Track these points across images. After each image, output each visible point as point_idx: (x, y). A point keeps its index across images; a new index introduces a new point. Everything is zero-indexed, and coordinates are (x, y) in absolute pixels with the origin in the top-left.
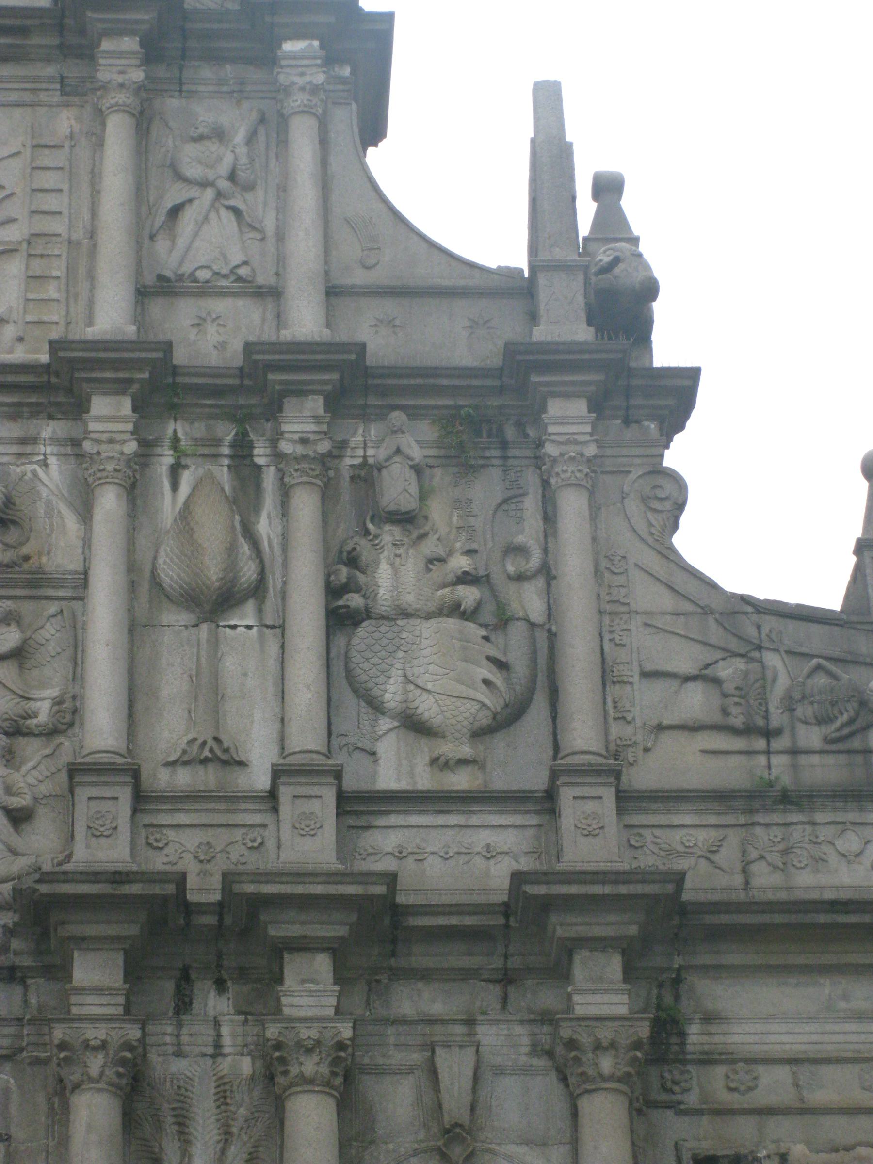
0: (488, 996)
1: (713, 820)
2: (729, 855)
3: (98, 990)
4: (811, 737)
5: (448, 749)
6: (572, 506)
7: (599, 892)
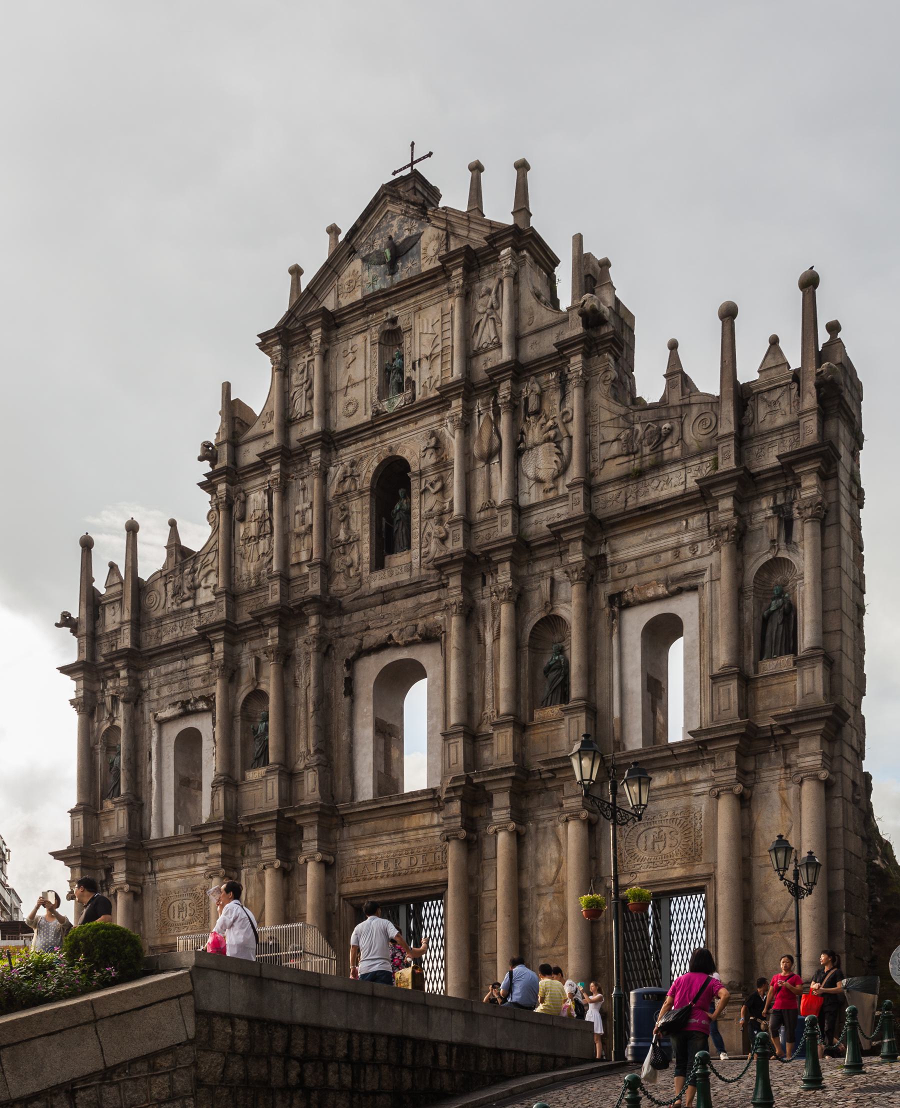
1: (617, 487)
2: (622, 497)
3: (455, 587)
5: (549, 485)
7: (570, 524)
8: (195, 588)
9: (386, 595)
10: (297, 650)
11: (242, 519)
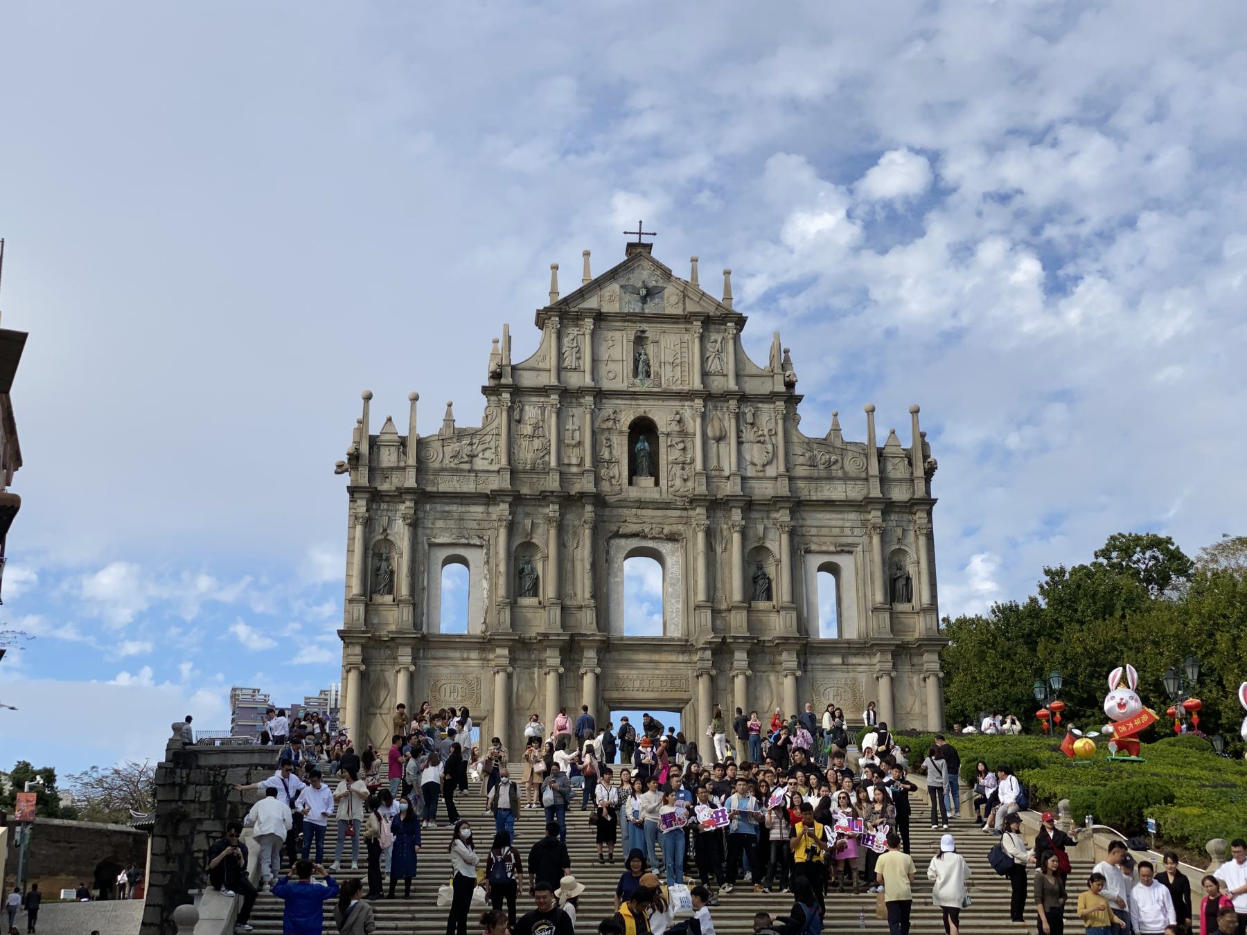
0: (765, 515)
4: (821, 467)
5: (759, 468)
8: (472, 457)
9: (641, 504)
10: (565, 522)
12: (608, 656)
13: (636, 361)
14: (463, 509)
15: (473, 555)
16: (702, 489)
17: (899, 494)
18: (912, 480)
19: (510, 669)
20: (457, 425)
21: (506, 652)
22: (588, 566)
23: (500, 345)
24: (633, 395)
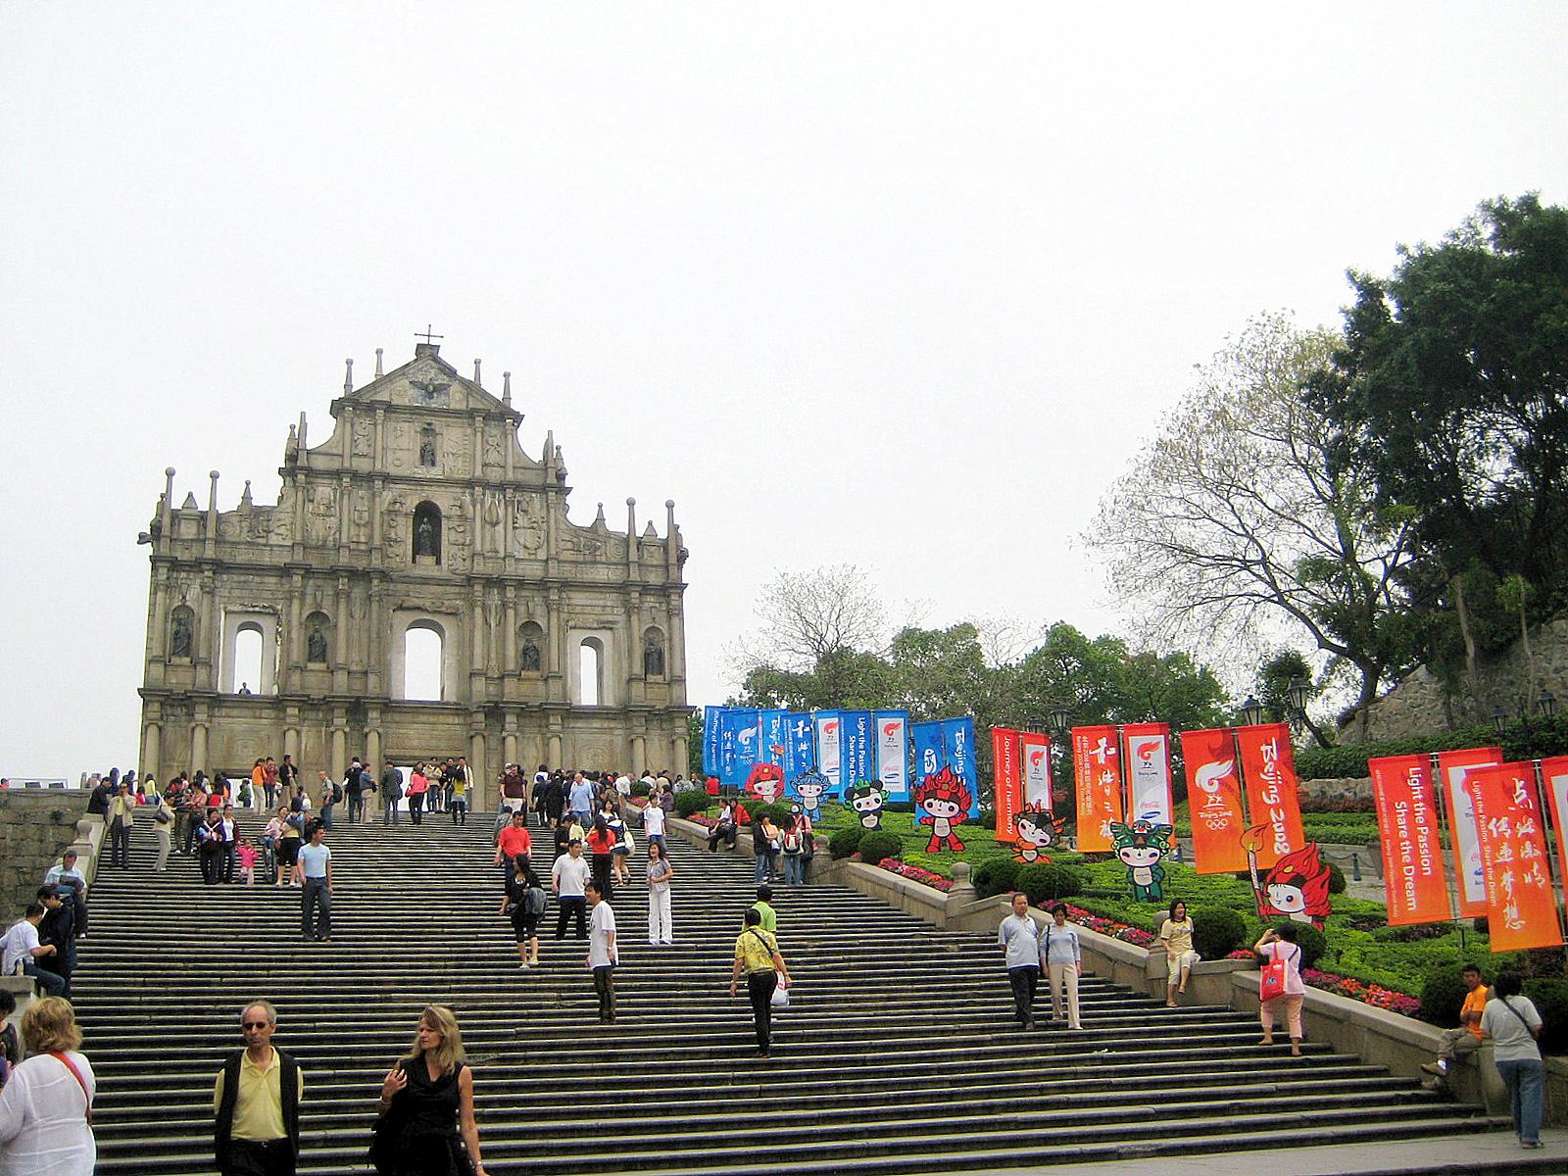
0: (536, 593)
4: (587, 552)
6: (552, 511)
9: (425, 581)
10: (353, 595)
11: (312, 501)
12: (389, 717)
13: (423, 451)
14: (257, 579)
15: (268, 623)
16: (480, 567)
17: (655, 578)
18: (667, 567)
19: (298, 728)
20: (254, 504)
21: (296, 711)
22: (374, 636)
23: (296, 431)
24: (419, 482)
